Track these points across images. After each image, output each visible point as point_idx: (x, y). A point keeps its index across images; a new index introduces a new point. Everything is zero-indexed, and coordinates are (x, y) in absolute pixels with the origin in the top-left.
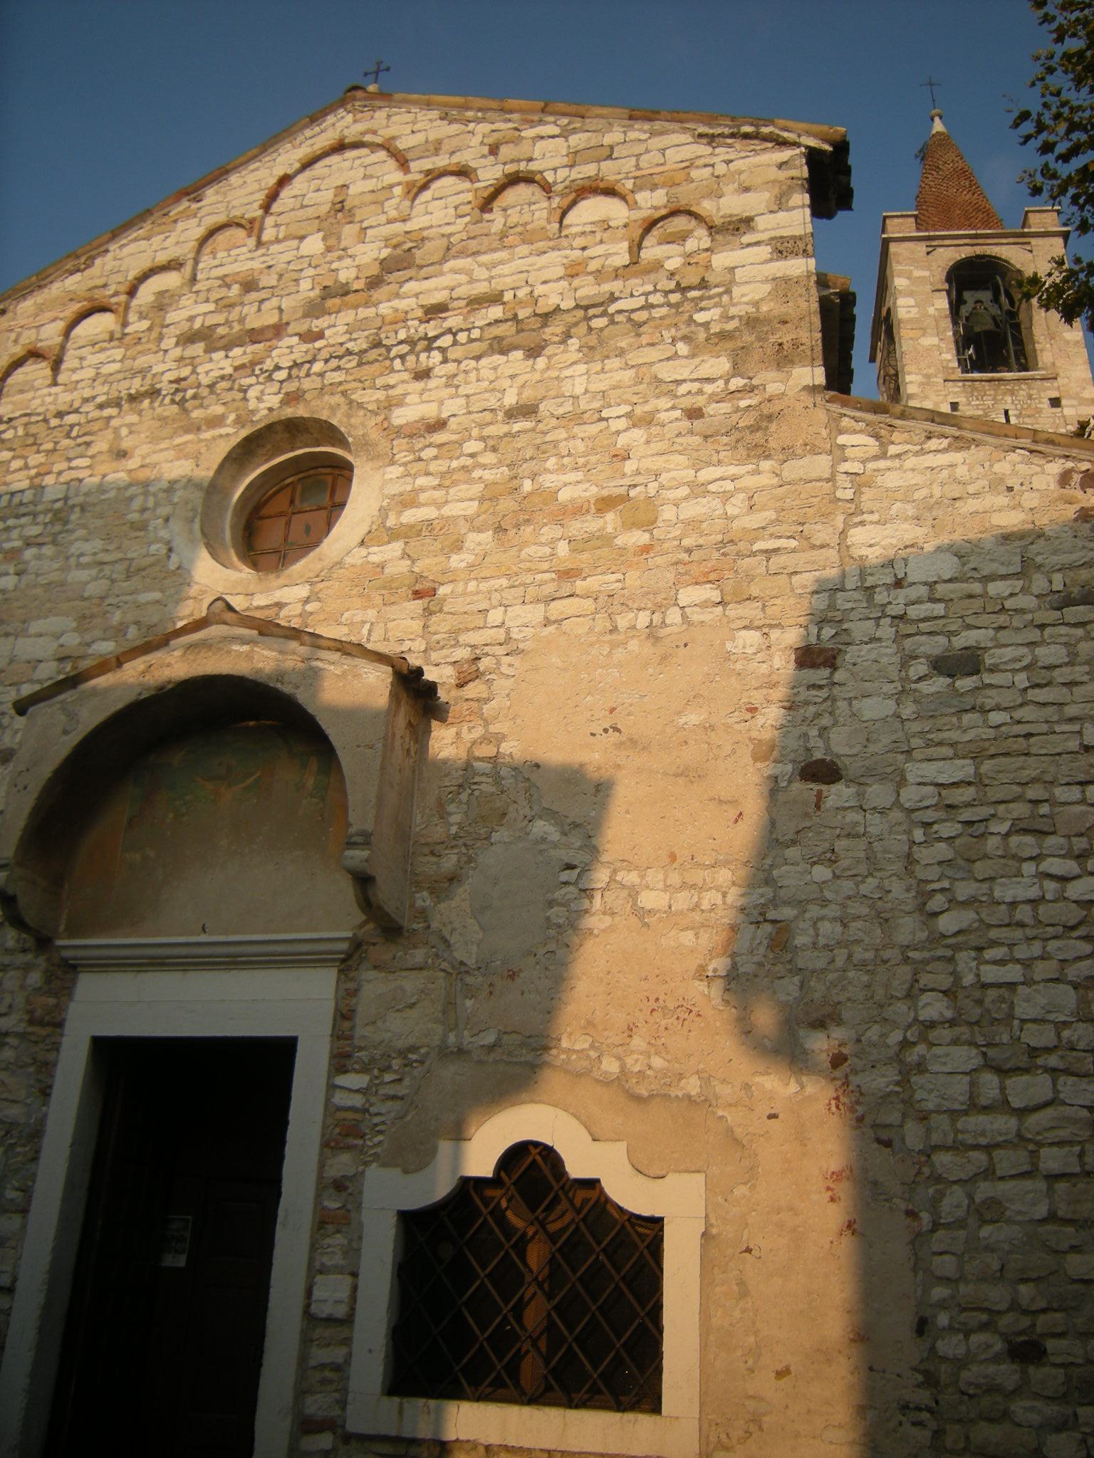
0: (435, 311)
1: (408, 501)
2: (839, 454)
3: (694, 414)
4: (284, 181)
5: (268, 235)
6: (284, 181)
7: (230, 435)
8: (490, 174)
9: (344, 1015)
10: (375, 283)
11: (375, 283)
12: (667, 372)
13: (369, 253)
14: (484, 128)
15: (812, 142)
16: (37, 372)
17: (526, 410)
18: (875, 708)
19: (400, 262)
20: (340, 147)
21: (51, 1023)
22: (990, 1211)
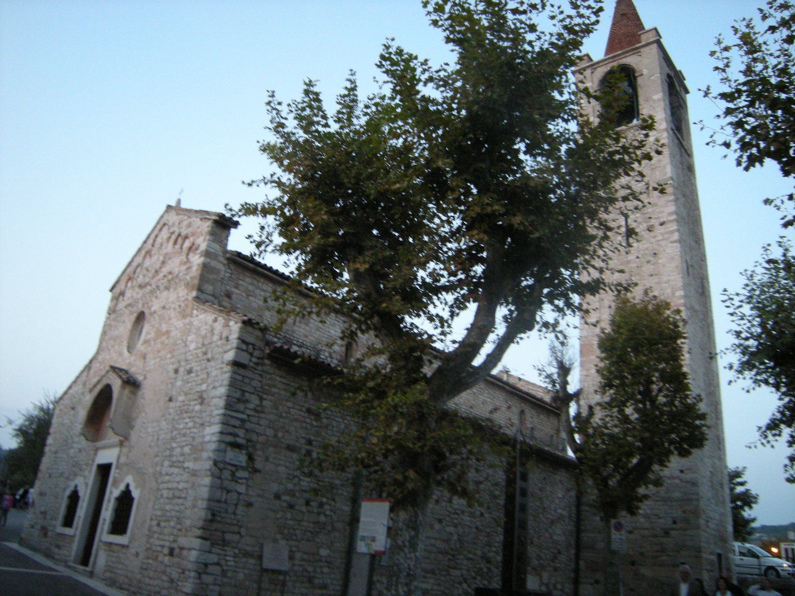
0: (165, 276)
1: (148, 333)
2: (191, 315)
3: (180, 306)
4: (157, 236)
5: (153, 253)
6: (157, 236)
7: (135, 315)
8: (176, 234)
9: (119, 457)
10: (161, 268)
11: (161, 268)
12: (181, 295)
13: (161, 258)
14: (180, 217)
15: (214, 218)
16: (121, 298)
17: (164, 308)
18: (179, 383)
19: (163, 263)
20: (165, 224)
21: (93, 461)
22: (162, 496)
